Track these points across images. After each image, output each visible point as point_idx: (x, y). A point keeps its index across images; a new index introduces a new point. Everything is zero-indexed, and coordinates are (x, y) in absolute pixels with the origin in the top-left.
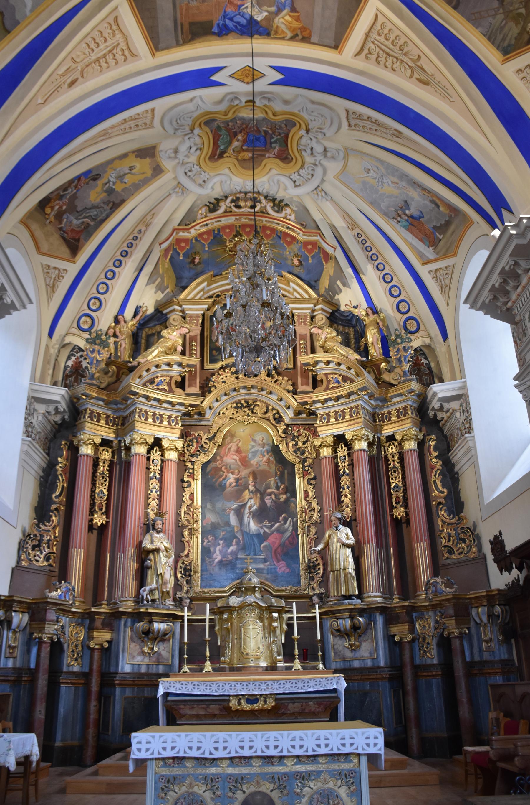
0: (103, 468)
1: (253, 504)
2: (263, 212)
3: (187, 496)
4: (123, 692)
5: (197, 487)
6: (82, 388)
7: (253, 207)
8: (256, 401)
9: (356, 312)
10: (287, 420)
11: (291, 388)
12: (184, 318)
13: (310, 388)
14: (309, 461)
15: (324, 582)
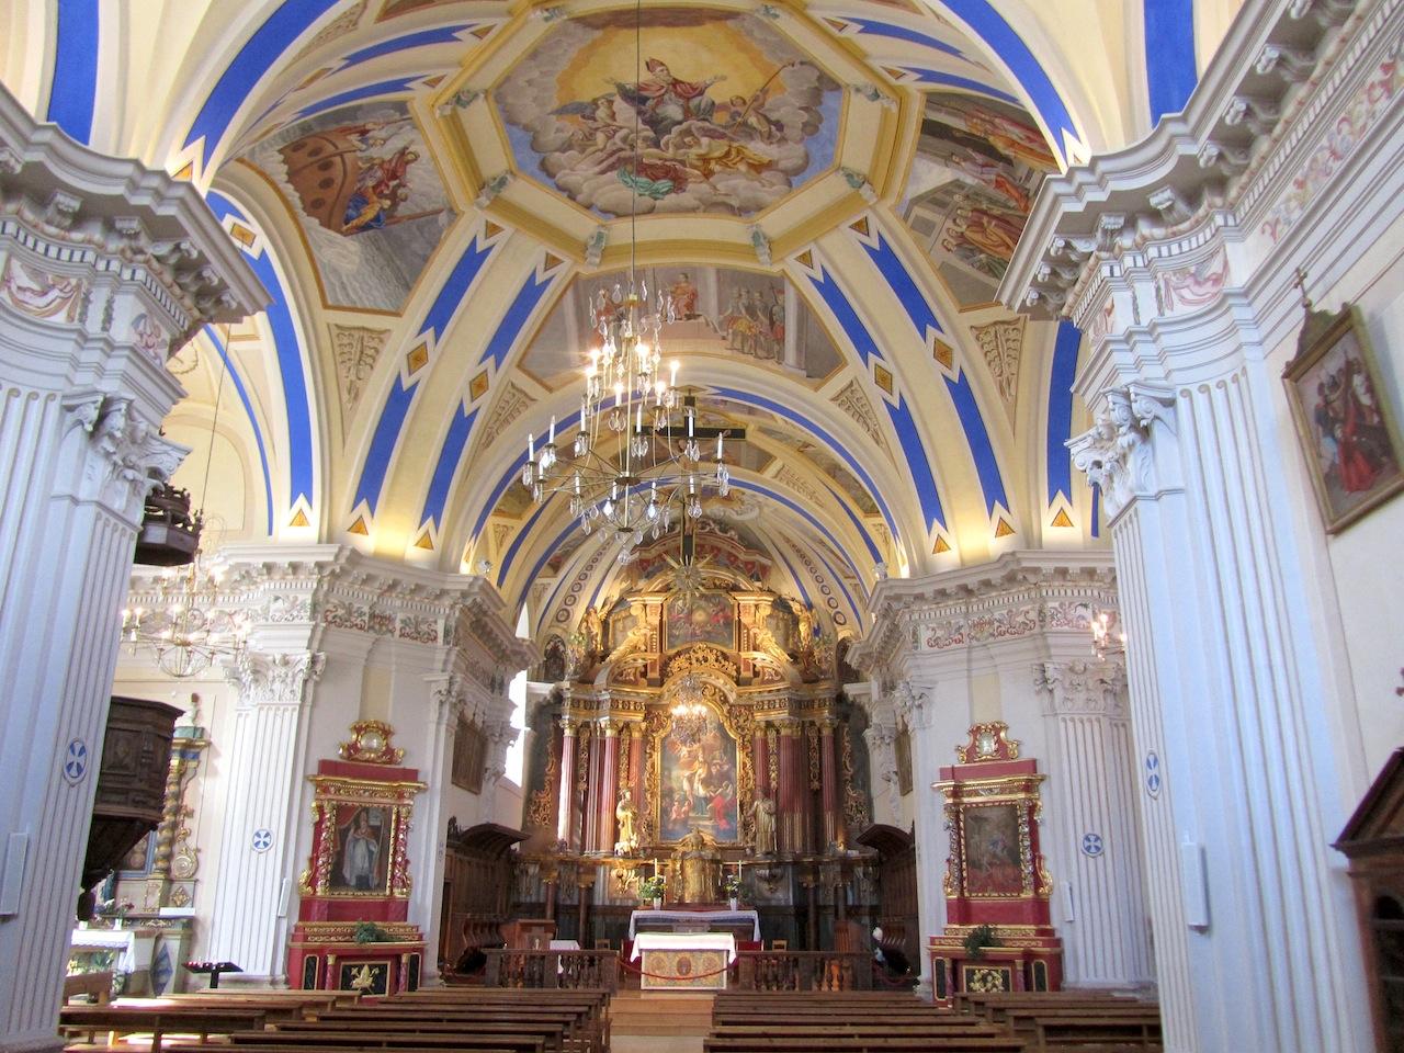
0: (583, 743)
1: (702, 772)
2: (712, 532)
3: (649, 764)
4: (604, 919)
5: (657, 757)
6: (566, 684)
7: (703, 528)
8: (705, 683)
9: (791, 603)
10: (731, 701)
11: (735, 674)
12: (645, 606)
13: (750, 674)
14: (748, 737)
15: (754, 839)
